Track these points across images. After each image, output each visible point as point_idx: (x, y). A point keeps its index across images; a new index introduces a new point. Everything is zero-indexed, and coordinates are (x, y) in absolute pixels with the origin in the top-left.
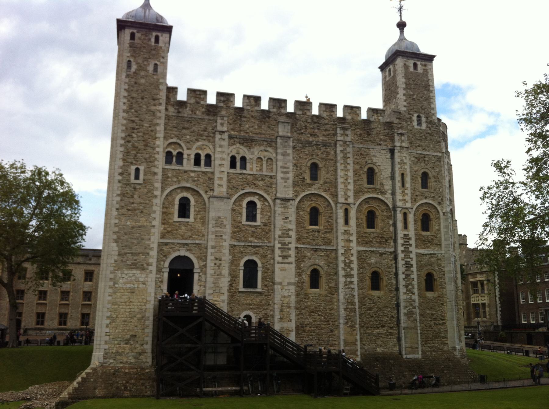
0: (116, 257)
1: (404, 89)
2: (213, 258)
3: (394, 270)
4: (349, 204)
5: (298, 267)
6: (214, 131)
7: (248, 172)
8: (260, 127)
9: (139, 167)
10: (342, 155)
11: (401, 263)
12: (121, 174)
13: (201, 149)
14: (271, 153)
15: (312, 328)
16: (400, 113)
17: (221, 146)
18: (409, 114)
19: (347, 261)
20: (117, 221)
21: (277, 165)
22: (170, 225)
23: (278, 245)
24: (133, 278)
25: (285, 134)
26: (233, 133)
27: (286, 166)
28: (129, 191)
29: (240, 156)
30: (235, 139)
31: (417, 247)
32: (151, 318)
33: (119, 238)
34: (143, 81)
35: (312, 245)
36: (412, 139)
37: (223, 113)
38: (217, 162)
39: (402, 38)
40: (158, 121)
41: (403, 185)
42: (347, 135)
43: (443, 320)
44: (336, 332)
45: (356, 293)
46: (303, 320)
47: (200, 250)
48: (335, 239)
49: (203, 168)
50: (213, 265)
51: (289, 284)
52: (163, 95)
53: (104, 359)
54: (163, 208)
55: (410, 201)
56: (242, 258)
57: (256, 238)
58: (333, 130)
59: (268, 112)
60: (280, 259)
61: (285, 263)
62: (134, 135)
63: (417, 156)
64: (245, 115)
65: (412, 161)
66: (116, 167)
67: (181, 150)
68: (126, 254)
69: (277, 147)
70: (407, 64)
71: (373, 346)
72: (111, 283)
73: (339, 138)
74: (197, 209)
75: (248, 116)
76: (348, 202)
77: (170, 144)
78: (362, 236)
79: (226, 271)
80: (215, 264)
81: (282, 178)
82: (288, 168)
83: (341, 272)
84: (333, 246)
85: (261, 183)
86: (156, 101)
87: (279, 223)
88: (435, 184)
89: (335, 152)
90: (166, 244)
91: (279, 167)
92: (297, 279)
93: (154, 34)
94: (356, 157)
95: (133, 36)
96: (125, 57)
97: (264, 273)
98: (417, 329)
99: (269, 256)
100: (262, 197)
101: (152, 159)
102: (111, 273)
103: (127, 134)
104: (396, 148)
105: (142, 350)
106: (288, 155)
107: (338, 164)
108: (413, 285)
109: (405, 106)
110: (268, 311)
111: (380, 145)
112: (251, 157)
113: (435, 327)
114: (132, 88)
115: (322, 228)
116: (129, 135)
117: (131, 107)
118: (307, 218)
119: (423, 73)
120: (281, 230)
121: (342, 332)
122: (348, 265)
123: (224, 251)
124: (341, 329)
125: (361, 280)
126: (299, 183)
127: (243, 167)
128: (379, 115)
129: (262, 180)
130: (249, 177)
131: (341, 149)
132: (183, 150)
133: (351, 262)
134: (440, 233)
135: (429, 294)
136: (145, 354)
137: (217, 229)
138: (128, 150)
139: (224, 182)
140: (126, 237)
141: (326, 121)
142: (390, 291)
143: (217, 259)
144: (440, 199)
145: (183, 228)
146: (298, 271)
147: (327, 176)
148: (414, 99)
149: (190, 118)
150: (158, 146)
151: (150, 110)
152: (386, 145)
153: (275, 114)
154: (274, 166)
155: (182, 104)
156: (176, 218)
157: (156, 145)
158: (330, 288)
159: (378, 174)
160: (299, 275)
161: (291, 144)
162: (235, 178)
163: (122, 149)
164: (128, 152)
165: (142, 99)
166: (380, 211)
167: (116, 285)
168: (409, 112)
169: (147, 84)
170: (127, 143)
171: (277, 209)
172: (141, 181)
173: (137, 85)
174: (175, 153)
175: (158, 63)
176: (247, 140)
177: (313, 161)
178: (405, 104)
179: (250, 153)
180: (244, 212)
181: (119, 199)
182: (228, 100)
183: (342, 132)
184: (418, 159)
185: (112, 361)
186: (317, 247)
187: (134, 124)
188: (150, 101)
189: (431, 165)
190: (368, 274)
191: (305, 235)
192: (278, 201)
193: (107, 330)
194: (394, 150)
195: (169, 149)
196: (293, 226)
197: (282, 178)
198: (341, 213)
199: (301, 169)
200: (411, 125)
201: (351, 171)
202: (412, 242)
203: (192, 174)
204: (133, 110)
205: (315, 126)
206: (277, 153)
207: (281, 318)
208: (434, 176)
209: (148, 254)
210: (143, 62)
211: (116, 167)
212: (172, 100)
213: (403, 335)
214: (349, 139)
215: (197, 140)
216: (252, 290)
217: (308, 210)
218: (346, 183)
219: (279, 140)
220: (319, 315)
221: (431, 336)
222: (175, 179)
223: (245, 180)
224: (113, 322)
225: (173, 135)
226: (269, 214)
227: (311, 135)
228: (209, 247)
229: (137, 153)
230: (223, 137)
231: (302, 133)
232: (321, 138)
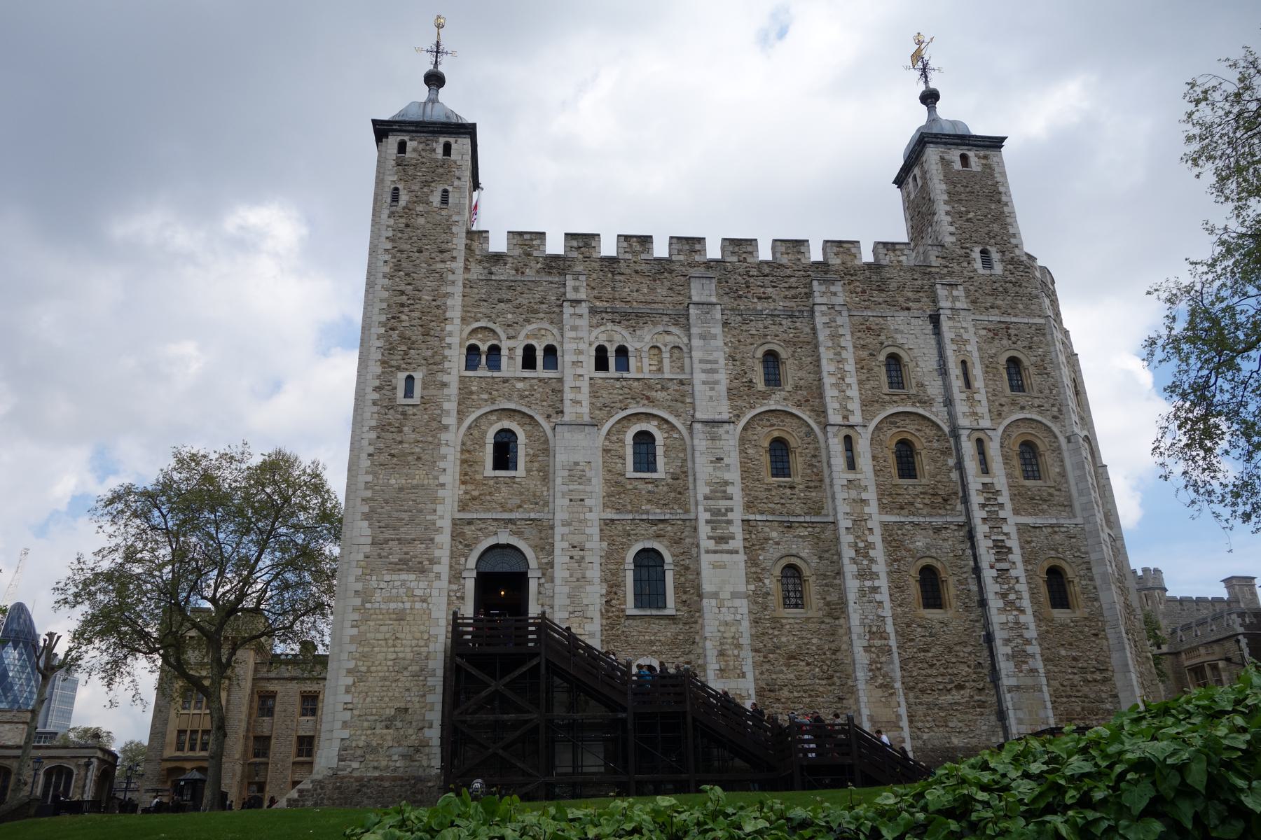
0: (367, 549)
1: (946, 203)
2: (566, 545)
3: (972, 563)
4: (852, 426)
5: (752, 561)
7: (633, 374)
10: (828, 331)
11: (983, 545)
12: (377, 389)
13: (535, 336)
15: (796, 694)
16: (943, 246)
19: (861, 545)
20: (369, 478)
22: (477, 485)
23: (704, 516)
24: (402, 591)
25: (704, 299)
26: (598, 304)
27: (710, 358)
28: (392, 421)
31: (1016, 512)
32: (440, 673)
33: (372, 510)
34: (421, 221)
37: (579, 268)
39: (933, 118)
40: (449, 289)
41: (968, 385)
42: (835, 294)
43: (1101, 671)
44: (851, 701)
45: (887, 611)
46: (774, 676)
47: (541, 531)
48: (830, 500)
49: (540, 372)
50: (567, 559)
51: (735, 595)
52: (460, 242)
53: (340, 760)
54: (462, 451)
55: (987, 416)
56: (629, 547)
57: (657, 504)
59: (669, 260)
60: (711, 544)
61: (722, 552)
62: (404, 317)
63: (992, 327)
65: (980, 337)
68: (386, 541)
70: (947, 157)
71: (940, 732)
72: (358, 601)
73: (818, 300)
74: (532, 452)
75: (627, 271)
77: (475, 331)
78: (890, 494)
79: (594, 573)
80: (571, 558)
81: (704, 383)
82: (716, 362)
83: (850, 569)
84: (827, 515)
85: (660, 395)
87: (703, 469)
88: (1038, 379)
89: (814, 329)
90: (470, 522)
91: (696, 361)
92: (752, 587)
93: (442, 140)
95: (402, 147)
97: (677, 574)
98: (1041, 691)
99: (687, 540)
100: (667, 421)
101: (438, 358)
102: (357, 580)
105: (421, 741)
106: (714, 337)
107: (822, 350)
110: (692, 657)
111: (908, 309)
112: (638, 345)
113: (1086, 689)
116: (393, 318)
117: (398, 267)
120: (707, 484)
121: (864, 700)
122: (863, 552)
123: (588, 531)
124: (861, 693)
125: (897, 587)
126: (740, 391)
129: (663, 389)
130: (636, 383)
133: (870, 546)
134: (1067, 482)
135: (1060, 614)
136: (427, 750)
137: (571, 487)
139: (584, 396)
141: (789, 272)
142: (967, 608)
143: (574, 547)
144: (1055, 409)
145: (504, 489)
146: (754, 570)
147: (800, 374)
148: (968, 220)
151: (434, 271)
154: (687, 361)
155: (498, 258)
156: (489, 470)
158: (828, 604)
159: (911, 365)
160: (755, 576)
161: (719, 316)
162: (605, 388)
163: (380, 343)
165: (420, 251)
166: (923, 440)
167: (368, 605)
168: (964, 244)
169: (429, 226)
171: (696, 442)
172: (416, 400)
174: (484, 347)
175: (450, 189)
176: (625, 316)
177: (767, 347)
178: (952, 229)
180: (629, 451)
181: (373, 435)
182: (587, 245)
183: (823, 288)
185: (355, 765)
186: (791, 519)
187: (405, 298)
189: (1025, 344)
190: (914, 572)
192: (697, 426)
193: (348, 698)
195: (472, 342)
196: (734, 475)
197: (704, 383)
198: (836, 445)
199: (743, 364)
201: (851, 361)
202: (1004, 498)
203: (520, 385)
204: (402, 273)
205: (767, 281)
207: (721, 670)
208: (1035, 365)
209: (432, 540)
212: (477, 252)
213: (1010, 705)
215: (528, 321)
216: (654, 612)
217: (766, 444)
220: (808, 664)
221: (1079, 709)
222: (485, 396)
223: (627, 391)
224: (361, 681)
226: (681, 455)
227: (760, 298)
228: (557, 523)
230: (578, 310)
231: (740, 297)
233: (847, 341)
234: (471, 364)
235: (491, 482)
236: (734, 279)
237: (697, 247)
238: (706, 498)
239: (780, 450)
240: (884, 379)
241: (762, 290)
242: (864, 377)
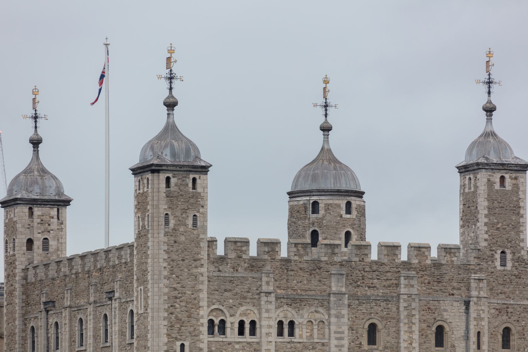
1: (486, 216)
6: (258, 292)
8: (309, 281)
9: (184, 342)
10: (406, 313)
14: (323, 315)
17: (267, 311)
18: (490, 250)
21: (329, 329)
26: (279, 291)
27: (340, 330)
30: (282, 300)
34: (183, 238)
36: (494, 284)
37: (268, 267)
38: (264, 331)
40: (201, 287)
41: (479, 347)
42: (412, 286)
49: (247, 338)
58: (396, 280)
62: (177, 306)
64: (293, 268)
66: (161, 344)
67: (223, 318)
69: (329, 307)
70: (492, 179)
77: (212, 311)
81: (336, 346)
82: (343, 333)
86: (197, 262)
88: (520, 341)
89: (398, 309)
91: (332, 332)
93: (192, 176)
94: (423, 312)
96: (162, 210)
101: (196, 332)
103: (170, 305)
104: (471, 299)
107: (402, 325)
109: (486, 240)
111: (453, 295)
112: (301, 320)
114: (171, 249)
116: (172, 306)
117: (172, 272)
119: (512, 190)
127: (291, 334)
128: (452, 255)
130: (298, 345)
131: (405, 305)
132: (226, 318)
138: (171, 323)
141: (387, 268)
147: (388, 339)
148: (498, 229)
149: (232, 277)
150: (202, 317)
151: (192, 274)
152: (460, 295)
153: (328, 264)
155: (222, 259)
157: (200, 316)
159: (450, 333)
161: (346, 302)
165: (183, 260)
170: (171, 315)
173: (176, 244)
174: (217, 322)
175: (197, 214)
176: (294, 300)
178: (486, 236)
179: (299, 317)
182: (273, 250)
184: (499, 311)
187: (177, 292)
188: (191, 263)
189: (516, 318)
194: (470, 301)
195: (211, 317)
197: (336, 346)
199: (357, 333)
200: (493, 266)
201: (417, 332)
203: (237, 346)
204: (174, 276)
205: (374, 275)
210: (182, 214)
211: (161, 344)
212: (211, 256)
214: (414, 291)
215: (241, 305)
219: (332, 298)
225: (214, 301)
227: (369, 287)
229: (181, 326)
231: (358, 286)
232: (381, 291)
233: (416, 320)
234: (211, 331)
240: (434, 342)
241: (371, 281)
242: (422, 341)
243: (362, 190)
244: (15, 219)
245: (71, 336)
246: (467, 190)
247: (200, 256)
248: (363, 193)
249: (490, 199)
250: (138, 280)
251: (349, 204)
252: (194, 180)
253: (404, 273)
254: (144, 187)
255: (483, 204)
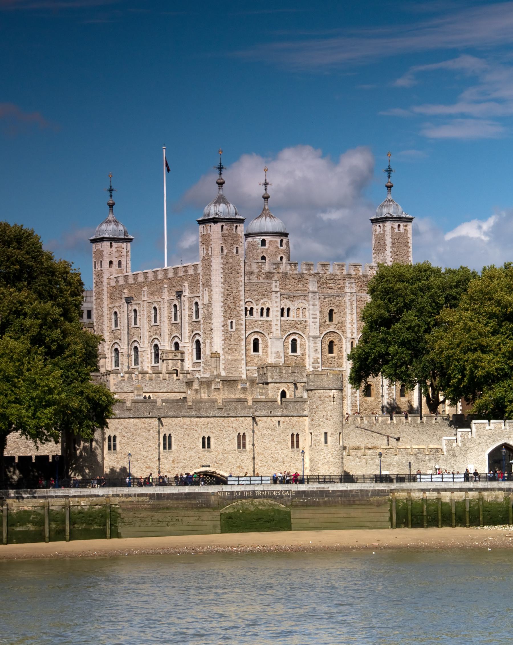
1: (391, 247)
3: (381, 383)
4: (354, 338)
12: (223, 326)
17: (276, 302)
26: (282, 291)
27: (315, 313)
29: (287, 307)
34: (231, 260)
35: (331, 367)
37: (276, 277)
40: (241, 288)
62: (229, 299)
76: (353, 337)
81: (313, 322)
85: (299, 326)
93: (235, 225)
94: (358, 303)
100: (301, 335)
108: (393, 393)
115: (336, 355)
118: (327, 349)
120: (314, 359)
129: (300, 324)
130: (293, 322)
131: (349, 298)
139: (279, 328)
140: (229, 366)
147: (340, 318)
151: (236, 281)
156: (252, 353)
164: (226, 311)
172: (234, 330)
174: (249, 309)
176: (290, 296)
178: (391, 259)
183: (349, 285)
191: (326, 361)
192: (311, 338)
196: (319, 356)
197: (313, 322)
203: (260, 323)
206: (309, 305)
215: (262, 299)
218: (352, 324)
219: (311, 295)
222: (250, 327)
233: (354, 306)
235: (253, 356)
236: (323, 281)
237: (312, 268)
238: (313, 363)
239: (331, 344)
243: (287, 232)
244: (101, 249)
245: (149, 317)
246: (377, 233)
247: (240, 271)
248: (288, 234)
249: (393, 237)
250: (203, 284)
251: (282, 241)
252: (236, 227)
253: (347, 280)
254: (207, 231)
255: (389, 240)
